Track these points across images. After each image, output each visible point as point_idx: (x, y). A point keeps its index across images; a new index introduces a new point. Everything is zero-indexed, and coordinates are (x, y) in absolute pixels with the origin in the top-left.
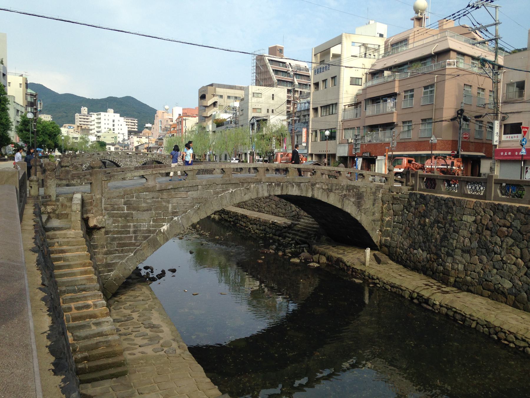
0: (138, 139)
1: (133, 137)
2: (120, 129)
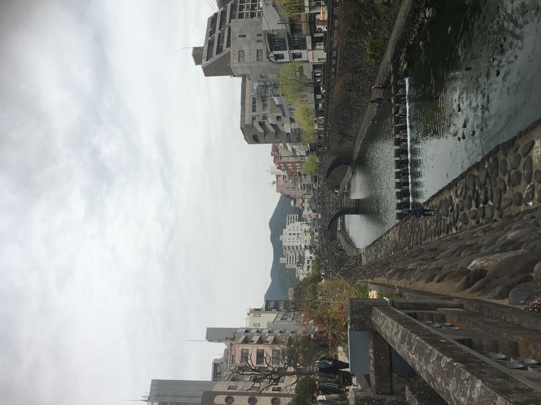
0: (306, 210)
1: (303, 214)
2: (297, 229)
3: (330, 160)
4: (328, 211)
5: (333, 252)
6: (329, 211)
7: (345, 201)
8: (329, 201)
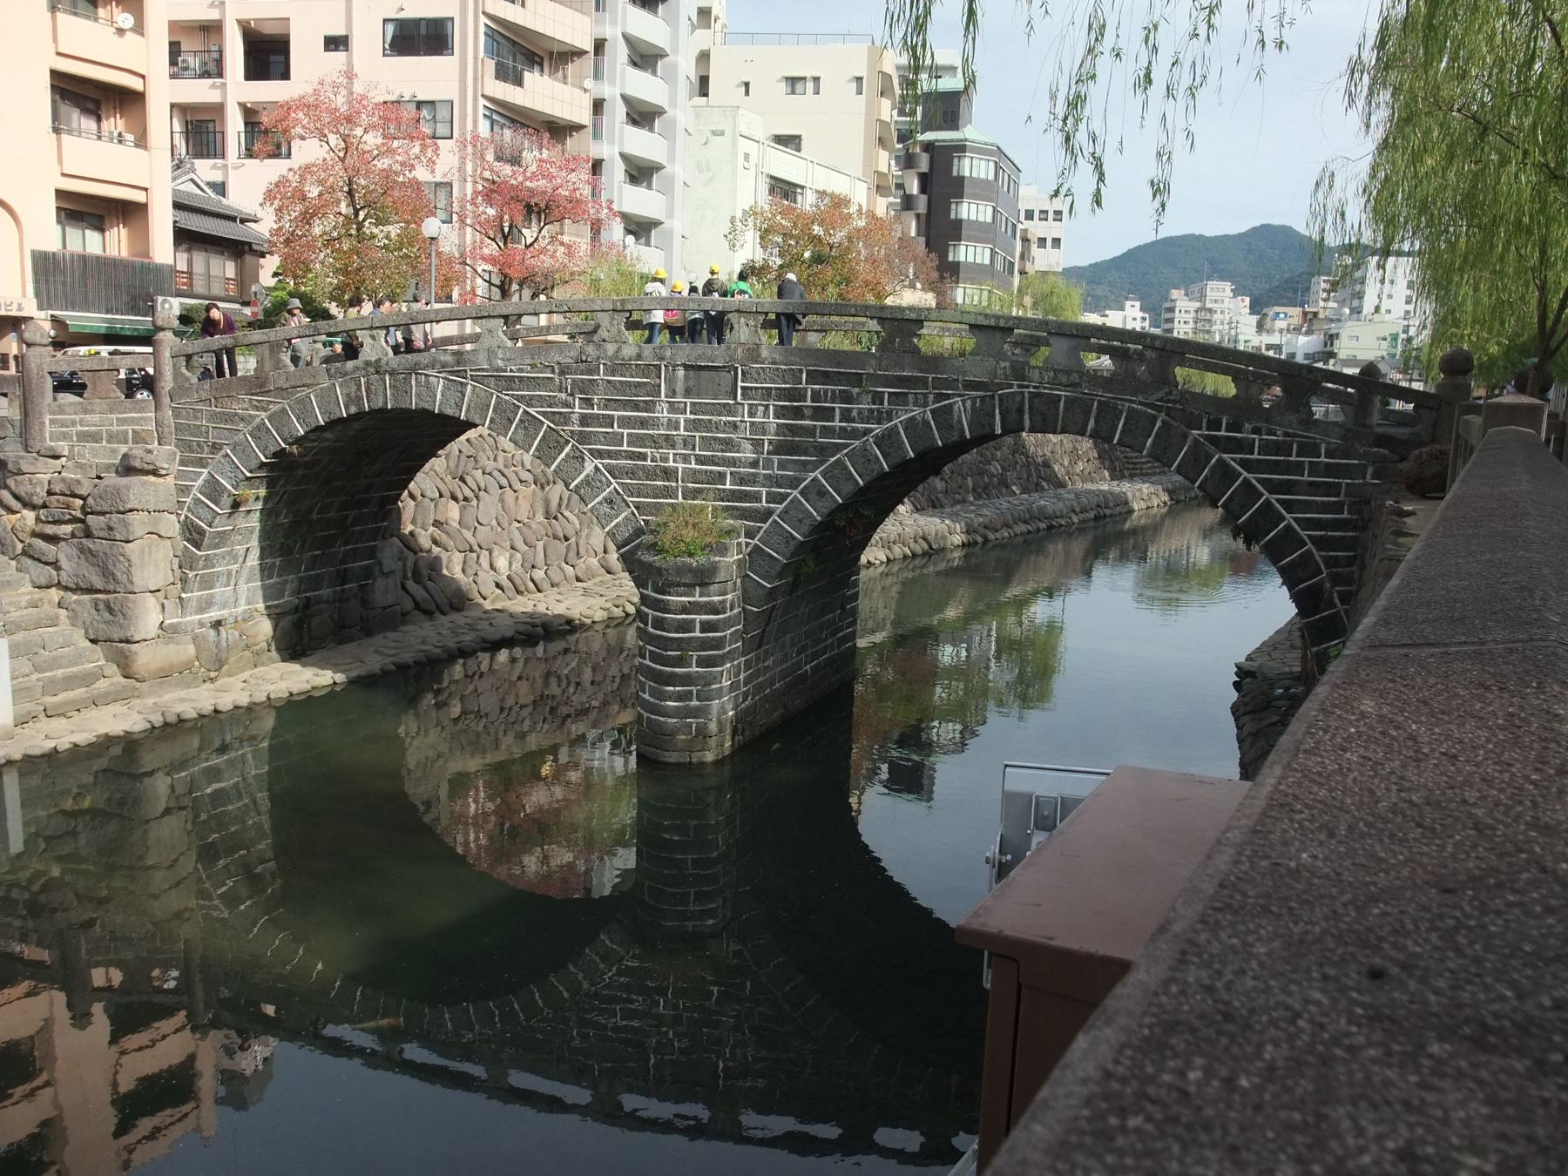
3: (1273, 487)
4: (625, 422)
5: (216, 448)
6: (618, 440)
7: (686, 626)
8: (729, 445)
